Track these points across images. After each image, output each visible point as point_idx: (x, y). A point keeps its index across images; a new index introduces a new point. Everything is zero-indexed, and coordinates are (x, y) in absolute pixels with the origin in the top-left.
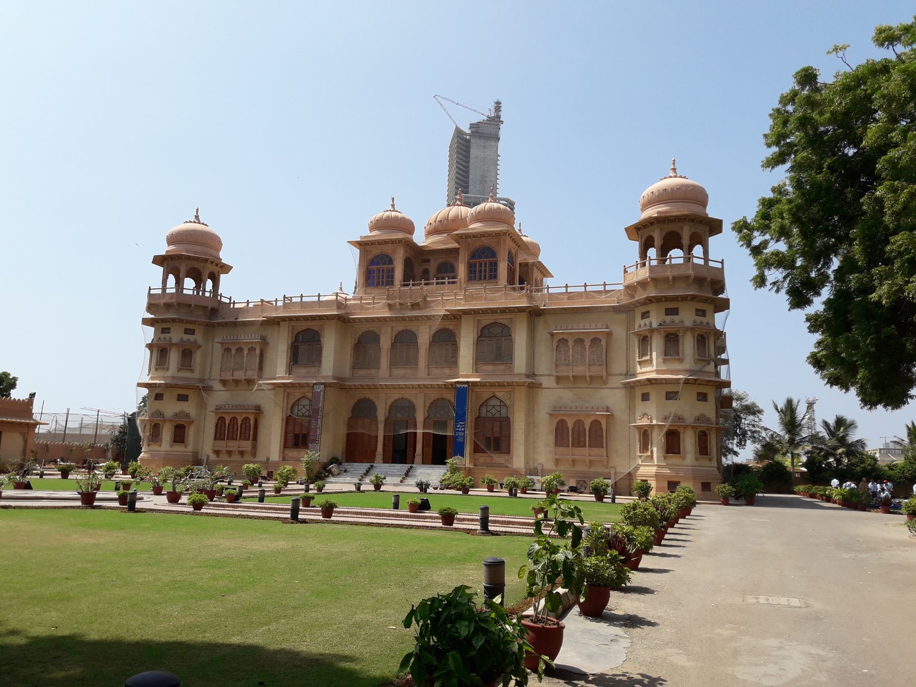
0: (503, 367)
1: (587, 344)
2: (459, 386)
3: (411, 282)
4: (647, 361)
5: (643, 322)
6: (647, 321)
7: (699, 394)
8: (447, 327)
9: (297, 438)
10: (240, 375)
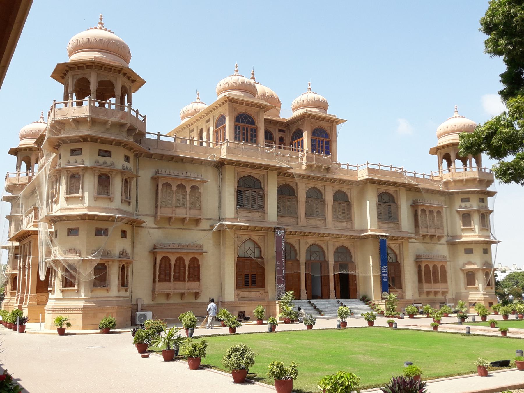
0: (392, 225)
1: (435, 214)
2: (381, 238)
3: (282, 146)
4: (472, 229)
5: (463, 204)
6: (468, 204)
7: (484, 249)
8: (316, 186)
9: (250, 276)
10: (181, 213)
